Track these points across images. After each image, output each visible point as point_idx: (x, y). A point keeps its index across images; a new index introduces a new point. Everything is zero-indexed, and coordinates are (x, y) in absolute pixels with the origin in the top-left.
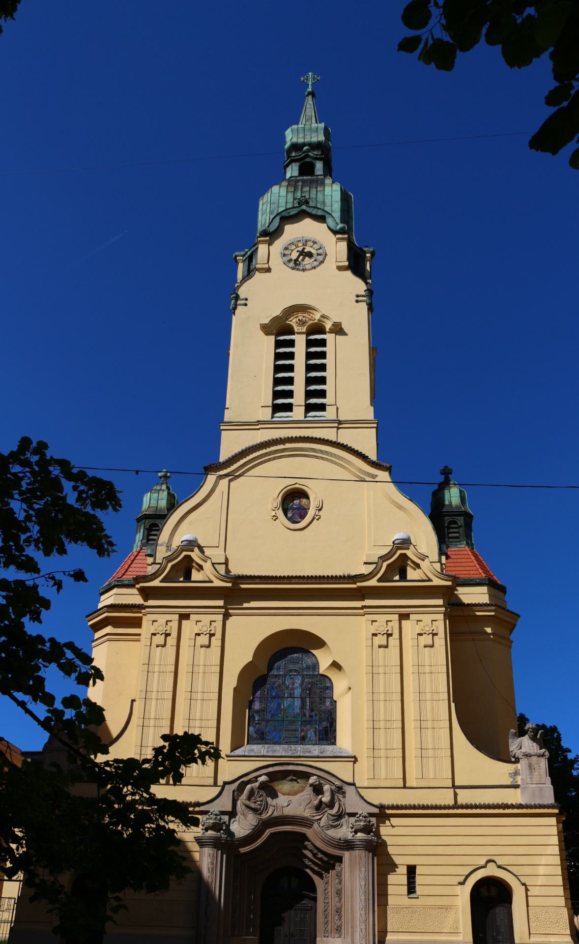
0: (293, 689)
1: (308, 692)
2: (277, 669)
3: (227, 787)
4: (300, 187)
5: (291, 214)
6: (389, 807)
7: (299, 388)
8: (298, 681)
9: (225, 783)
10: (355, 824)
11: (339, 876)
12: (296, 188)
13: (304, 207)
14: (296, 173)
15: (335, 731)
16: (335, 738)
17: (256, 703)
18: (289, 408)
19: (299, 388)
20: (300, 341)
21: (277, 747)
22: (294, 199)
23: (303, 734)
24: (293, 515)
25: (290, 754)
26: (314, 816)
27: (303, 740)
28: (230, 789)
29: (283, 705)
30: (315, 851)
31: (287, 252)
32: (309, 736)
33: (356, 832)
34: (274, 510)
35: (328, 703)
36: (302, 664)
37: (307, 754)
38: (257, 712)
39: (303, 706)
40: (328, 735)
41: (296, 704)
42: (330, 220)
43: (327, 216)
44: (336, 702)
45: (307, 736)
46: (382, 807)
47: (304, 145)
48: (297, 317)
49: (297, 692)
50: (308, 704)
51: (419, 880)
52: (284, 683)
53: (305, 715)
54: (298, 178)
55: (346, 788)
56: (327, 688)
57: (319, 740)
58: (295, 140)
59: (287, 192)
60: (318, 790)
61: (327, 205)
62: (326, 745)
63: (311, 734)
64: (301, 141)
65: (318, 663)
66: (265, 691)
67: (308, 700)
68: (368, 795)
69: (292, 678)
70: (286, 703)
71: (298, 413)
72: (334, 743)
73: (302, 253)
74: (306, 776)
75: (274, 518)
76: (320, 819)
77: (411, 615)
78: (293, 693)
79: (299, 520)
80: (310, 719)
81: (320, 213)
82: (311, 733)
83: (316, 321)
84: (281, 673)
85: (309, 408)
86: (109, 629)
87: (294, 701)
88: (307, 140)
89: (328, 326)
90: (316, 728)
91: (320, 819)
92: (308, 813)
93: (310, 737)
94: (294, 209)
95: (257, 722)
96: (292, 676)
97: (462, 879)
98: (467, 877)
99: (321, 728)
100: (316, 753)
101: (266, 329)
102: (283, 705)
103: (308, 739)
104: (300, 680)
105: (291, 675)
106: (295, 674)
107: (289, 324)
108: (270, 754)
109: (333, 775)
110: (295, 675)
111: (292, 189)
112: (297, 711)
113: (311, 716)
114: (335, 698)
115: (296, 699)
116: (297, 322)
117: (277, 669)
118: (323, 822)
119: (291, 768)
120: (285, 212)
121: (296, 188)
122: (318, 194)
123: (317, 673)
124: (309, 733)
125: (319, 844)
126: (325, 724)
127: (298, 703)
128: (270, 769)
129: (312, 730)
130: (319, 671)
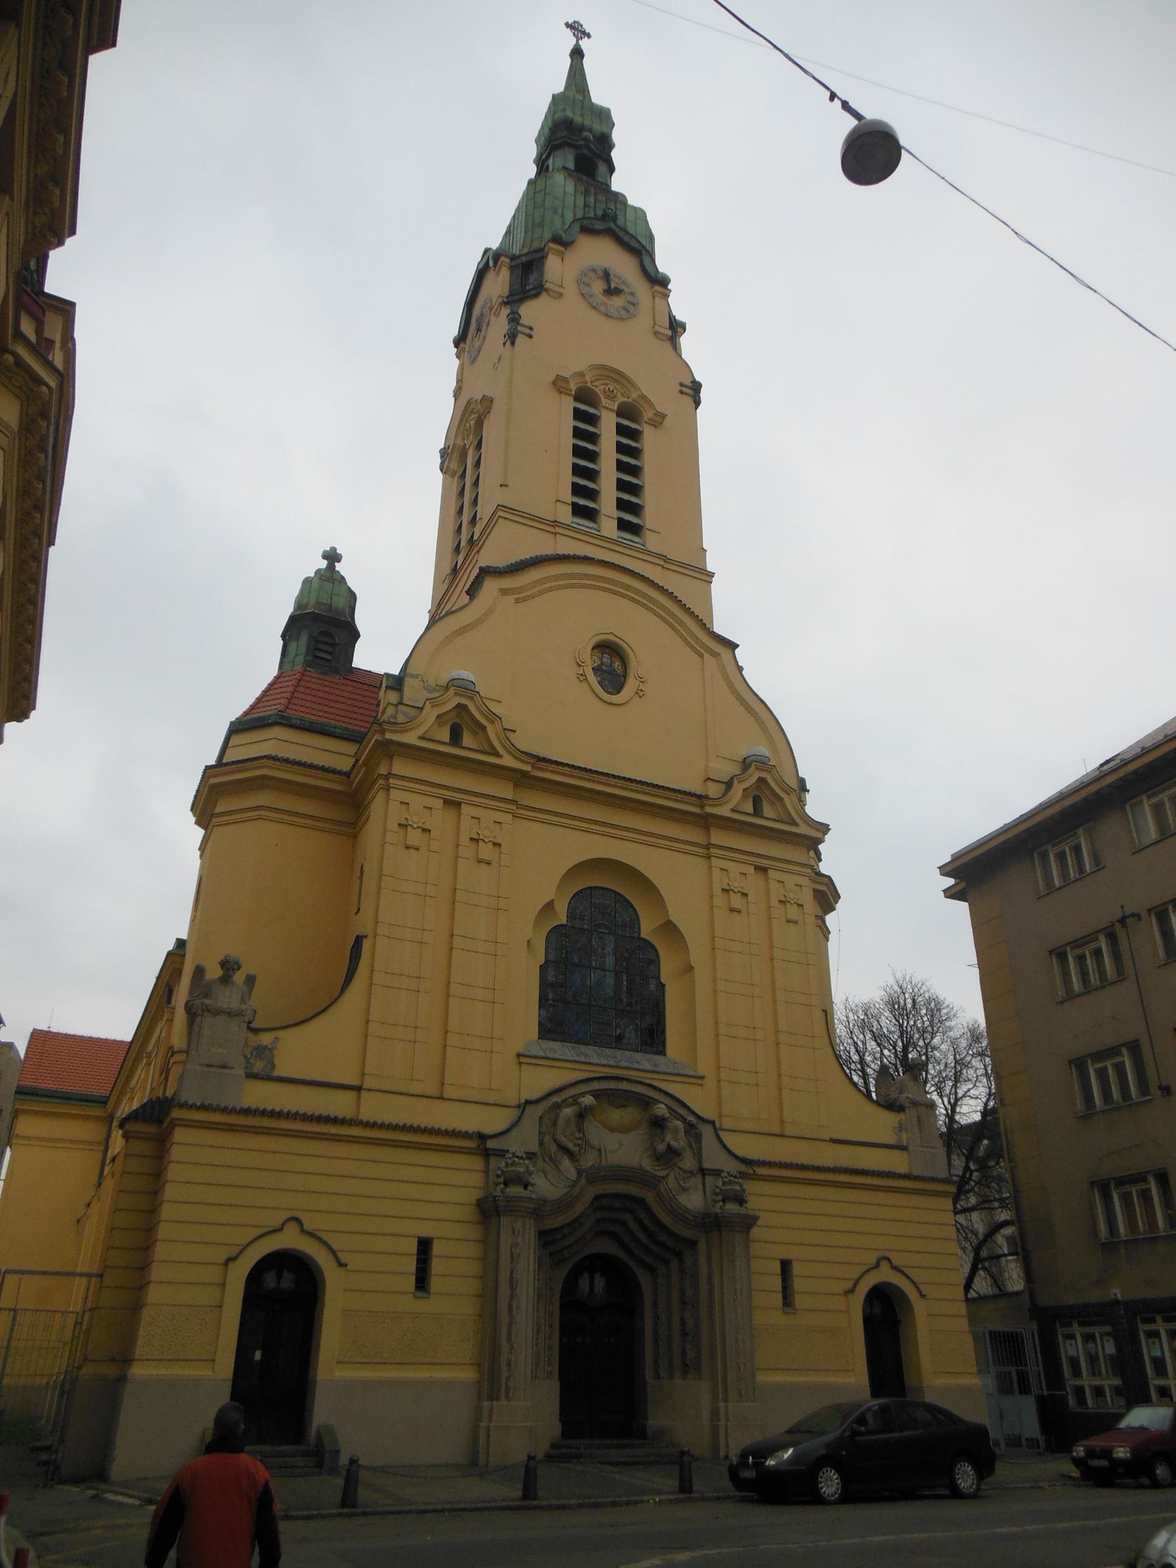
1: (624, 964)
2: (580, 919)
3: (530, 1110)
4: (593, 191)
7: (608, 494)
8: (610, 941)
9: (528, 1102)
10: (723, 1188)
15: (663, 1032)
16: (663, 1043)
17: (549, 969)
19: (608, 494)
21: (583, 1048)
23: (618, 1031)
25: (612, 1062)
26: (655, 1170)
27: (618, 1042)
28: (535, 1112)
29: (588, 979)
31: (586, 280)
32: (627, 1036)
34: (580, 666)
35: (652, 987)
36: (616, 918)
37: (636, 1066)
38: (552, 985)
41: (607, 982)
43: (643, 252)
44: (663, 986)
45: (624, 1036)
46: (744, 1161)
48: (607, 385)
49: (610, 961)
50: (625, 983)
52: (590, 942)
53: (621, 1001)
56: (650, 962)
58: (569, 114)
59: (575, 189)
62: (651, 1053)
63: (631, 1035)
65: (638, 919)
66: (563, 954)
67: (625, 978)
68: (730, 1140)
69: (601, 938)
70: (595, 976)
71: (609, 527)
72: (662, 1052)
74: (645, 1103)
75: (582, 678)
76: (667, 1176)
77: (769, 871)
78: (604, 962)
80: (629, 1008)
82: (630, 1032)
84: (586, 927)
86: (263, 798)
87: (605, 975)
90: (637, 1025)
91: (667, 1176)
92: (647, 1164)
93: (628, 1038)
95: (551, 1002)
96: (603, 935)
97: (850, 1285)
98: (857, 1281)
100: (648, 1067)
101: (559, 384)
102: (588, 979)
103: (625, 1041)
104: (613, 943)
105: (601, 933)
106: (606, 931)
107: (595, 391)
108: (583, 1059)
110: (604, 933)
112: (610, 992)
113: (630, 1005)
114: (663, 980)
115: (607, 973)
116: (605, 392)
117: (580, 919)
119: (624, 1086)
123: (636, 935)
124: (628, 1030)
127: (610, 980)
128: (596, 1086)
129: (631, 1027)
130: (639, 934)
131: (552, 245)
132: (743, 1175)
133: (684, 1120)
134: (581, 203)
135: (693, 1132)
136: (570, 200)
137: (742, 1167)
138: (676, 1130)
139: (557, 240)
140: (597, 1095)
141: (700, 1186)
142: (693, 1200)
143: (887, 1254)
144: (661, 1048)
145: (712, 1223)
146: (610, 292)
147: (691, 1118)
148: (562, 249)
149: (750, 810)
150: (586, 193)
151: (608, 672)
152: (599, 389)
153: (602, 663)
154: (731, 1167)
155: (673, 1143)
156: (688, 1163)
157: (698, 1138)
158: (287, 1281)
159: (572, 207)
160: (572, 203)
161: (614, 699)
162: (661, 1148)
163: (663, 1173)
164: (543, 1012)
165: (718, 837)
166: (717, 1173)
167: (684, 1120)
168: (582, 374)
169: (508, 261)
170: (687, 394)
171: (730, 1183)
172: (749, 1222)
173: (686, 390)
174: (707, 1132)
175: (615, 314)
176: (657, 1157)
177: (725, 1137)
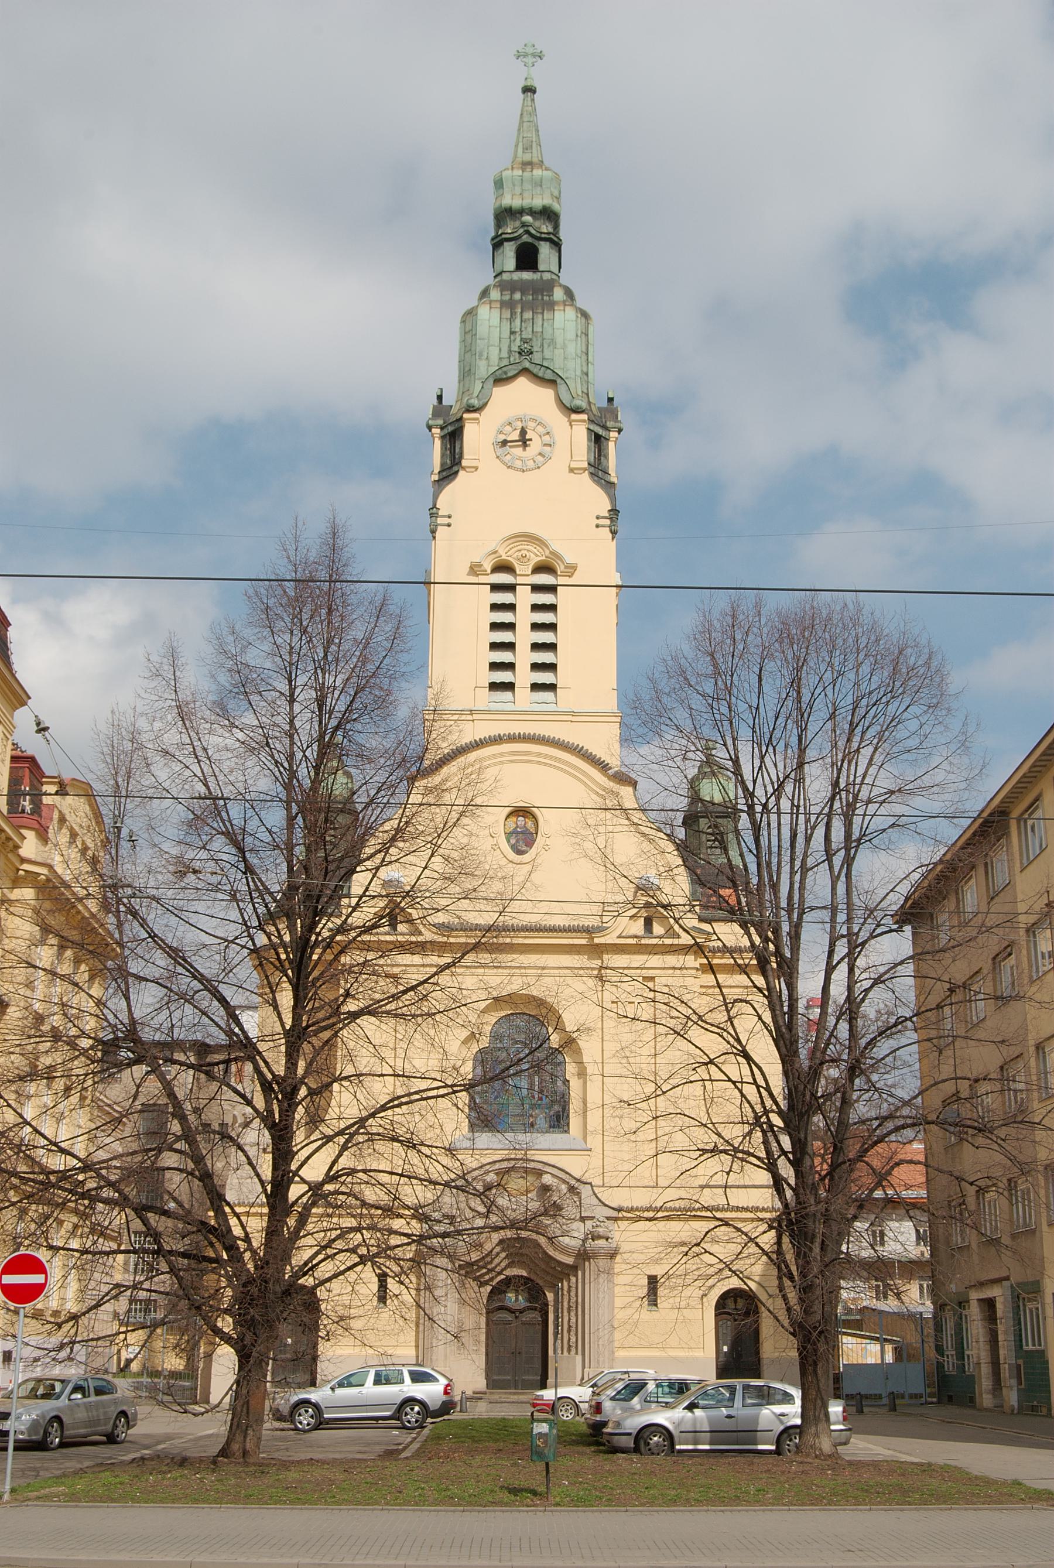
5: (510, 374)
13: (527, 364)
18: (509, 686)
22: (512, 333)
24: (517, 841)
35: (559, 1083)
40: (559, 1121)
42: (562, 388)
43: (559, 381)
47: (521, 212)
53: (533, 1097)
56: (559, 1064)
57: (550, 1127)
61: (558, 346)
63: (541, 1122)
64: (516, 203)
72: (567, 1131)
79: (524, 848)
81: (549, 375)
83: (544, 558)
88: (527, 202)
89: (560, 568)
94: (513, 367)
99: (552, 1113)
111: (507, 314)
122: (545, 324)
126: (557, 1108)
131: (465, 416)
134: (506, 333)
139: (471, 409)
144: (566, 1128)
145: (584, 1256)
146: (524, 441)
147: (573, 1182)
150: (512, 319)
151: (521, 832)
154: (602, 1212)
159: (497, 343)
160: (497, 335)
169: (438, 431)
170: (603, 526)
172: (613, 1255)
173: (602, 522)
174: (586, 1191)
175: (531, 464)
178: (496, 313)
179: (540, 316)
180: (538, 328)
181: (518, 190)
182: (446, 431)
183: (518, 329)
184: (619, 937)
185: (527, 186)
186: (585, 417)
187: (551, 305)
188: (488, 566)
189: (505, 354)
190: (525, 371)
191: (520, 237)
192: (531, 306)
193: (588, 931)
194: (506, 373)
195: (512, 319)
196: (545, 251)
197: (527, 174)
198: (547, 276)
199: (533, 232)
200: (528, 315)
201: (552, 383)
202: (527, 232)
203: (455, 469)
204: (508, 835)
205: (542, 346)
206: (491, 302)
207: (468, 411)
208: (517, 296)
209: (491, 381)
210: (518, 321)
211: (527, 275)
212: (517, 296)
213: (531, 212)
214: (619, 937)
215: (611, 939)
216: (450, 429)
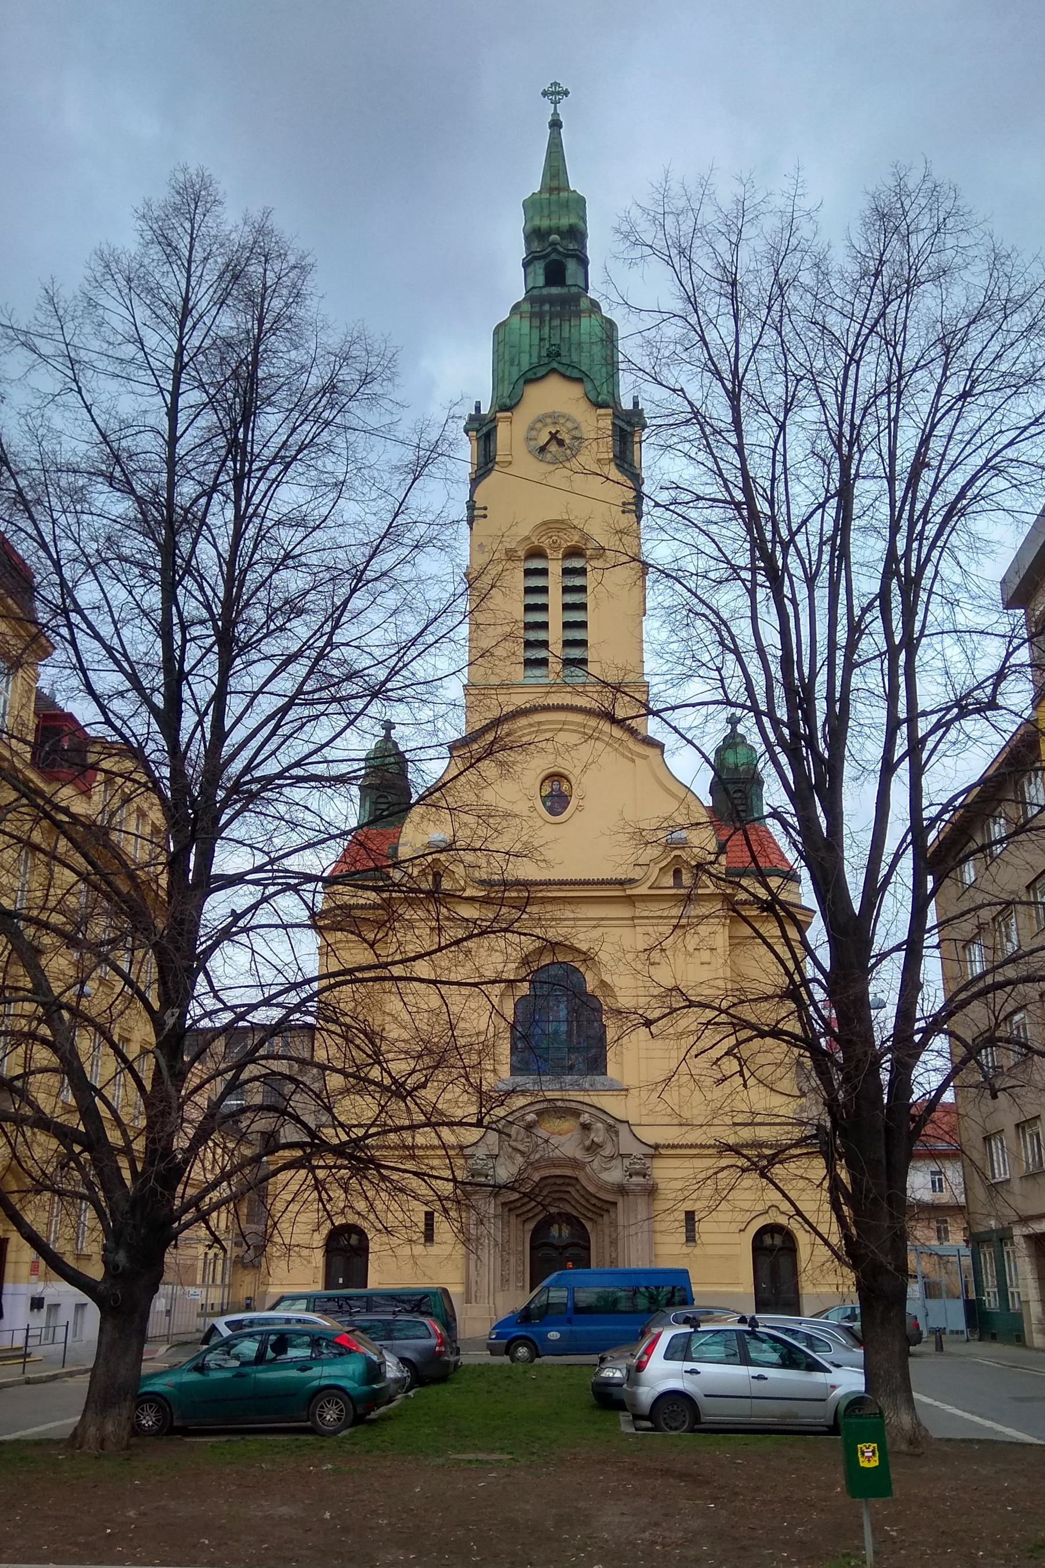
0: (558, 1012)
5: (539, 375)
6: (668, 1146)
11: (614, 1224)
12: (542, 322)
13: (555, 365)
14: (541, 281)
18: (543, 662)
20: (555, 568)
22: (541, 339)
30: (588, 1197)
33: (631, 1176)
39: (569, 1034)
40: (597, 1064)
43: (585, 379)
47: (550, 232)
48: (551, 537)
49: (563, 1014)
51: (700, 1227)
54: (545, 291)
55: (619, 1126)
60: (586, 1127)
67: (575, 1024)
73: (553, 436)
74: (576, 1113)
81: (576, 374)
85: (568, 662)
88: (554, 222)
92: (579, 1154)
109: (605, 1112)
118: (595, 1165)
120: (530, 373)
121: (542, 322)
125: (591, 1189)
127: (564, 1028)
131: (499, 415)
132: (653, 1157)
133: (604, 1122)
135: (612, 1130)
136: (526, 341)
137: (652, 1151)
138: (598, 1130)
140: (539, 1113)
141: (620, 1165)
142: (615, 1175)
143: (774, 1203)
147: (611, 1121)
148: (509, 414)
149: (671, 883)
150: (540, 328)
152: (545, 543)
153: (553, 790)
154: (638, 1150)
155: (595, 1139)
156: (608, 1151)
157: (617, 1133)
158: (778, 1240)
161: (558, 819)
162: (588, 1143)
163: (590, 1159)
164: (514, 1058)
165: (641, 910)
166: (629, 1155)
167: (604, 1122)
168: (527, 538)
171: (634, 1163)
174: (623, 1129)
176: (588, 1149)
177: (637, 1131)
178: (526, 323)
179: (567, 323)
180: (566, 335)
181: (546, 212)
182: (481, 433)
183: (546, 336)
184: (650, 888)
185: (554, 208)
186: (610, 411)
187: (578, 315)
188: (521, 554)
189: (535, 360)
190: (554, 371)
191: (548, 255)
192: (560, 316)
193: (621, 883)
194: (535, 374)
195: (540, 328)
196: (571, 266)
197: (554, 197)
198: (574, 290)
199: (561, 249)
200: (556, 322)
201: (579, 380)
202: (555, 250)
203: (490, 465)
204: (544, 799)
205: (570, 350)
206: (521, 313)
207: (501, 410)
208: (547, 307)
209: (521, 381)
210: (547, 329)
211: (555, 290)
212: (547, 307)
213: (558, 231)
214: (650, 888)
215: (643, 890)
216: (485, 430)
